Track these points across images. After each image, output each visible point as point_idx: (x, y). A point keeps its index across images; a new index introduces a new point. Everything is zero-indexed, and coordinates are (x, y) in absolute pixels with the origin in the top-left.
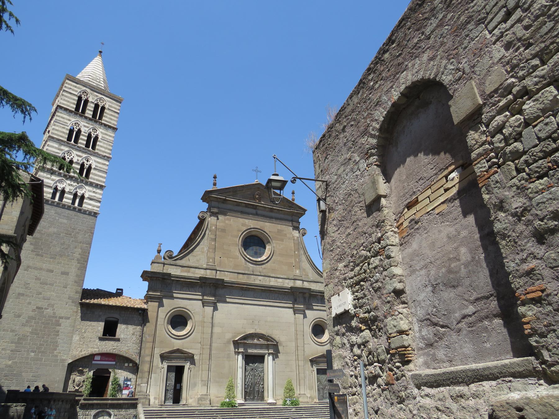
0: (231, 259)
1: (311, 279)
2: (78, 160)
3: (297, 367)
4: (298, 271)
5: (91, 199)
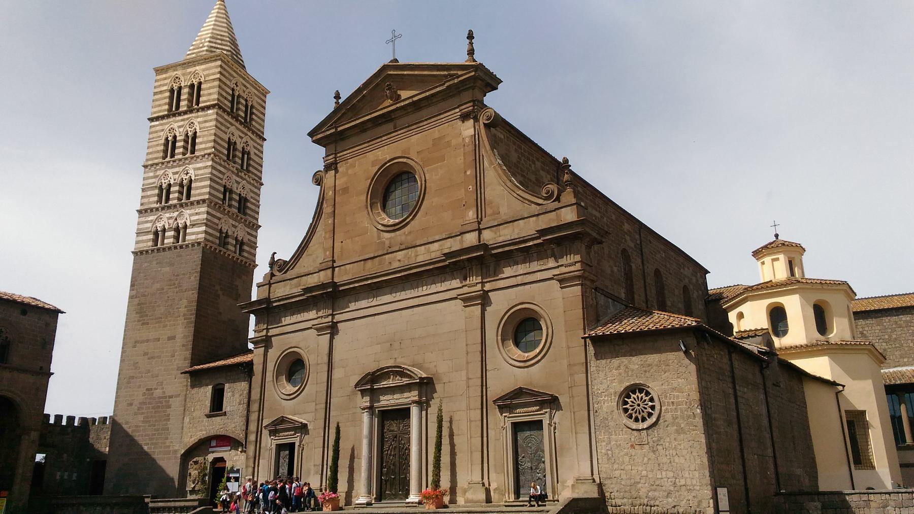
0: (357, 239)
2: (175, 180)
5: (193, 225)
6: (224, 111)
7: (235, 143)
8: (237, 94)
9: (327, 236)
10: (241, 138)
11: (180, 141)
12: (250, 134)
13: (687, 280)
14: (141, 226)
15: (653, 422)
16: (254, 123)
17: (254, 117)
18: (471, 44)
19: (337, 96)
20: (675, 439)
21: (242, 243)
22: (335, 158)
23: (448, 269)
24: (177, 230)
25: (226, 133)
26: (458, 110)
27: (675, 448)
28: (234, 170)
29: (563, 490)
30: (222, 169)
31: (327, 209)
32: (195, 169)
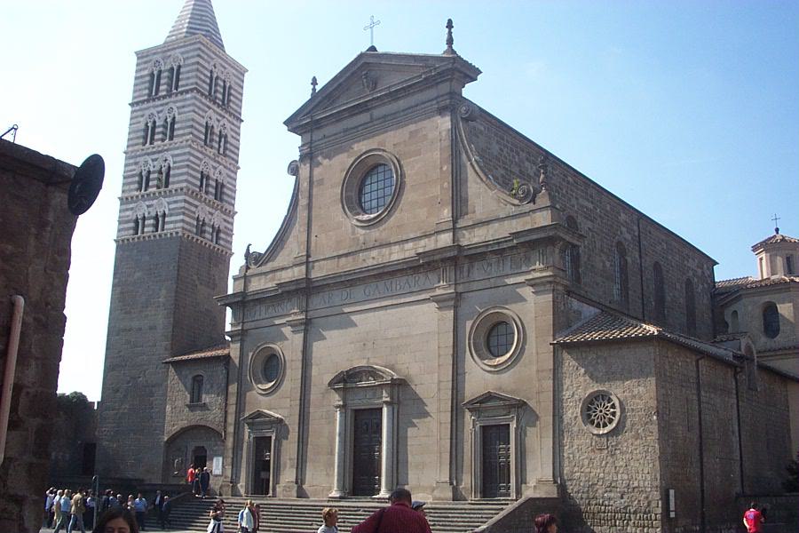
0: (331, 233)
2: (154, 167)
5: (171, 215)
6: (202, 94)
7: (213, 127)
8: (215, 75)
9: (302, 230)
10: (219, 121)
11: (159, 127)
12: (227, 116)
13: (691, 274)
14: (123, 214)
16: (231, 104)
17: (232, 98)
18: (450, 33)
19: (314, 82)
21: (219, 231)
22: (310, 148)
24: (156, 218)
25: (203, 117)
26: (434, 102)
28: (211, 155)
30: (200, 156)
31: (303, 202)
32: (173, 156)
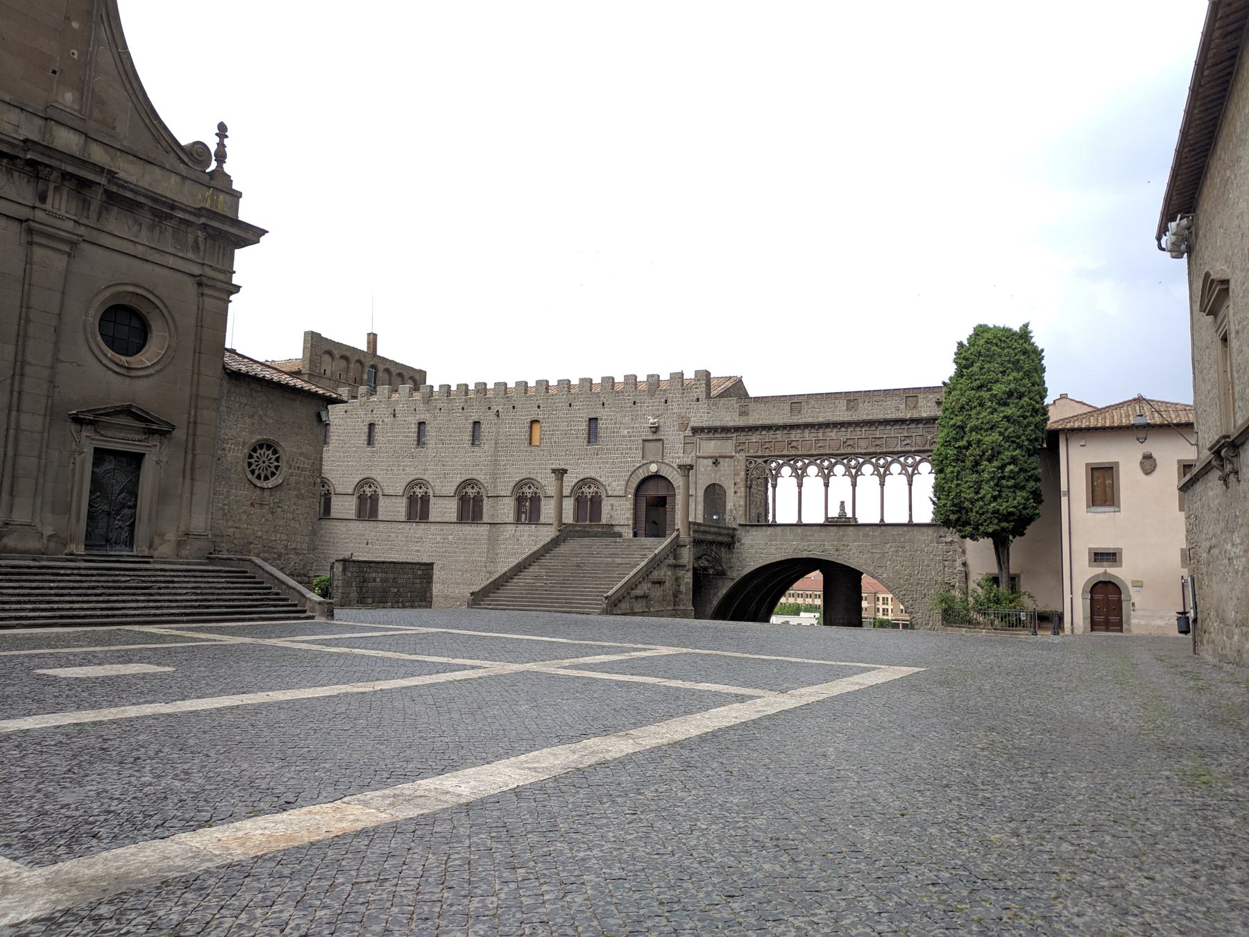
1: (126, 143)
3: (12, 432)
4: (69, 97)
15: (278, 483)
20: (294, 504)
23: (5, 161)
27: (293, 513)
29: (162, 544)
